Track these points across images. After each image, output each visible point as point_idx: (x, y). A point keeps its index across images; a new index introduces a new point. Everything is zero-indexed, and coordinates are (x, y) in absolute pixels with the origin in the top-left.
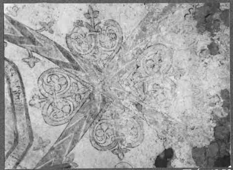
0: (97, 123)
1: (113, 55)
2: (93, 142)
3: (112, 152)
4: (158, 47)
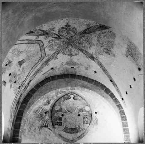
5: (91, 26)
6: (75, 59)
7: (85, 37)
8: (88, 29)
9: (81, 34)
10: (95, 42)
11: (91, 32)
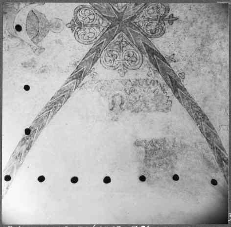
0: (95, 11)
1: (141, 30)
2: (81, 7)
3: (73, 20)
4: (141, 61)
5: (172, 64)
6: (67, 34)
7: (138, 55)
8: (164, 59)
9: (145, 45)
10: (131, 75)
11: (156, 66)
